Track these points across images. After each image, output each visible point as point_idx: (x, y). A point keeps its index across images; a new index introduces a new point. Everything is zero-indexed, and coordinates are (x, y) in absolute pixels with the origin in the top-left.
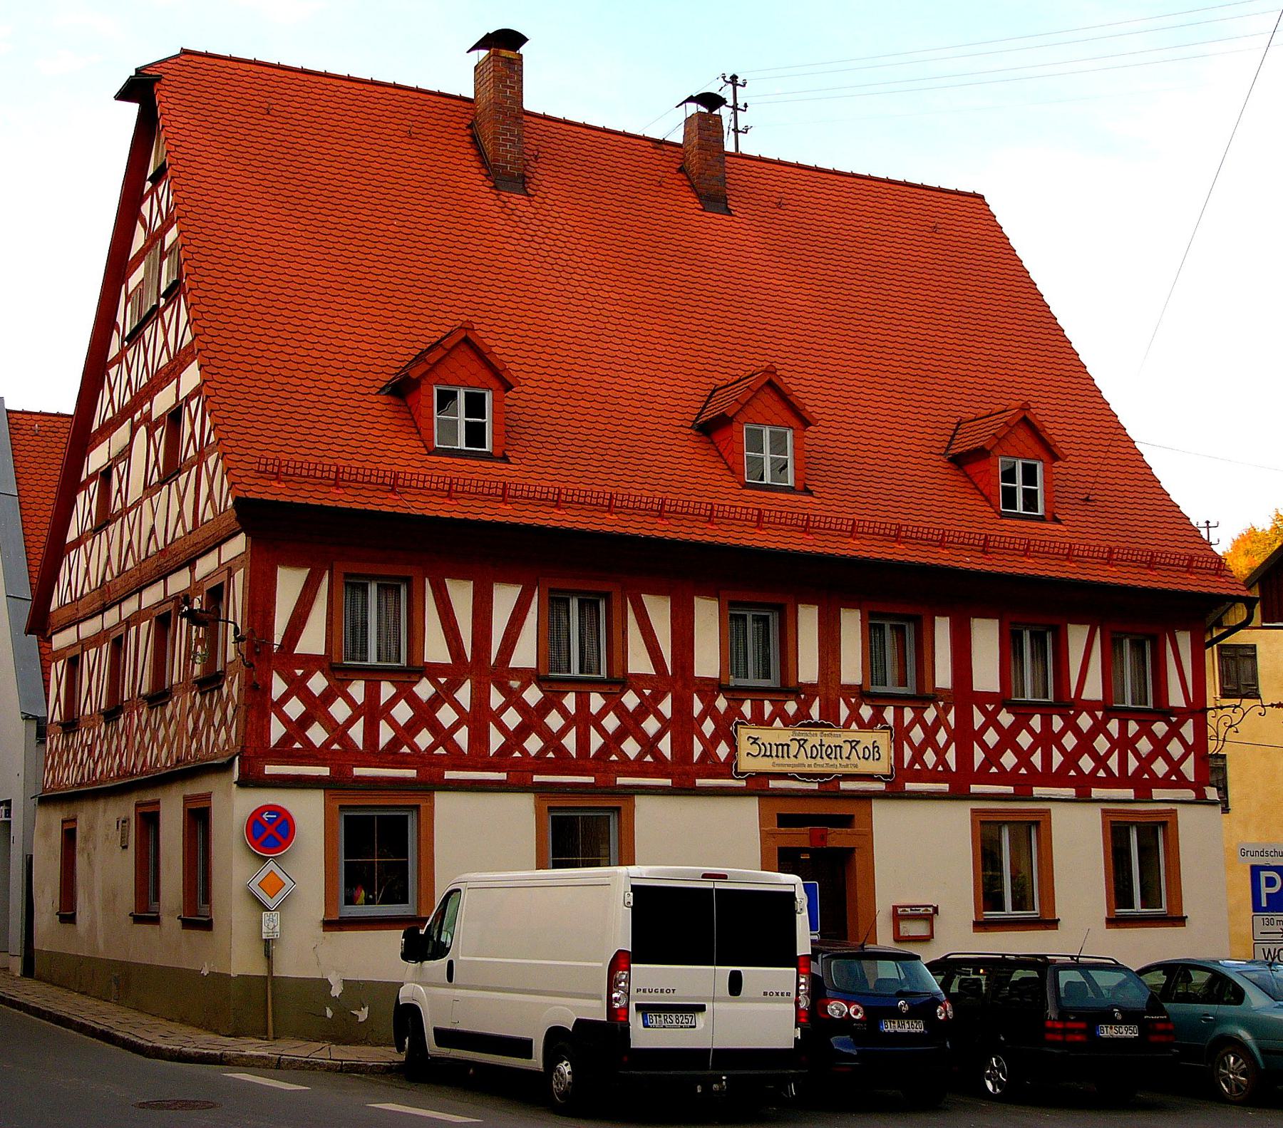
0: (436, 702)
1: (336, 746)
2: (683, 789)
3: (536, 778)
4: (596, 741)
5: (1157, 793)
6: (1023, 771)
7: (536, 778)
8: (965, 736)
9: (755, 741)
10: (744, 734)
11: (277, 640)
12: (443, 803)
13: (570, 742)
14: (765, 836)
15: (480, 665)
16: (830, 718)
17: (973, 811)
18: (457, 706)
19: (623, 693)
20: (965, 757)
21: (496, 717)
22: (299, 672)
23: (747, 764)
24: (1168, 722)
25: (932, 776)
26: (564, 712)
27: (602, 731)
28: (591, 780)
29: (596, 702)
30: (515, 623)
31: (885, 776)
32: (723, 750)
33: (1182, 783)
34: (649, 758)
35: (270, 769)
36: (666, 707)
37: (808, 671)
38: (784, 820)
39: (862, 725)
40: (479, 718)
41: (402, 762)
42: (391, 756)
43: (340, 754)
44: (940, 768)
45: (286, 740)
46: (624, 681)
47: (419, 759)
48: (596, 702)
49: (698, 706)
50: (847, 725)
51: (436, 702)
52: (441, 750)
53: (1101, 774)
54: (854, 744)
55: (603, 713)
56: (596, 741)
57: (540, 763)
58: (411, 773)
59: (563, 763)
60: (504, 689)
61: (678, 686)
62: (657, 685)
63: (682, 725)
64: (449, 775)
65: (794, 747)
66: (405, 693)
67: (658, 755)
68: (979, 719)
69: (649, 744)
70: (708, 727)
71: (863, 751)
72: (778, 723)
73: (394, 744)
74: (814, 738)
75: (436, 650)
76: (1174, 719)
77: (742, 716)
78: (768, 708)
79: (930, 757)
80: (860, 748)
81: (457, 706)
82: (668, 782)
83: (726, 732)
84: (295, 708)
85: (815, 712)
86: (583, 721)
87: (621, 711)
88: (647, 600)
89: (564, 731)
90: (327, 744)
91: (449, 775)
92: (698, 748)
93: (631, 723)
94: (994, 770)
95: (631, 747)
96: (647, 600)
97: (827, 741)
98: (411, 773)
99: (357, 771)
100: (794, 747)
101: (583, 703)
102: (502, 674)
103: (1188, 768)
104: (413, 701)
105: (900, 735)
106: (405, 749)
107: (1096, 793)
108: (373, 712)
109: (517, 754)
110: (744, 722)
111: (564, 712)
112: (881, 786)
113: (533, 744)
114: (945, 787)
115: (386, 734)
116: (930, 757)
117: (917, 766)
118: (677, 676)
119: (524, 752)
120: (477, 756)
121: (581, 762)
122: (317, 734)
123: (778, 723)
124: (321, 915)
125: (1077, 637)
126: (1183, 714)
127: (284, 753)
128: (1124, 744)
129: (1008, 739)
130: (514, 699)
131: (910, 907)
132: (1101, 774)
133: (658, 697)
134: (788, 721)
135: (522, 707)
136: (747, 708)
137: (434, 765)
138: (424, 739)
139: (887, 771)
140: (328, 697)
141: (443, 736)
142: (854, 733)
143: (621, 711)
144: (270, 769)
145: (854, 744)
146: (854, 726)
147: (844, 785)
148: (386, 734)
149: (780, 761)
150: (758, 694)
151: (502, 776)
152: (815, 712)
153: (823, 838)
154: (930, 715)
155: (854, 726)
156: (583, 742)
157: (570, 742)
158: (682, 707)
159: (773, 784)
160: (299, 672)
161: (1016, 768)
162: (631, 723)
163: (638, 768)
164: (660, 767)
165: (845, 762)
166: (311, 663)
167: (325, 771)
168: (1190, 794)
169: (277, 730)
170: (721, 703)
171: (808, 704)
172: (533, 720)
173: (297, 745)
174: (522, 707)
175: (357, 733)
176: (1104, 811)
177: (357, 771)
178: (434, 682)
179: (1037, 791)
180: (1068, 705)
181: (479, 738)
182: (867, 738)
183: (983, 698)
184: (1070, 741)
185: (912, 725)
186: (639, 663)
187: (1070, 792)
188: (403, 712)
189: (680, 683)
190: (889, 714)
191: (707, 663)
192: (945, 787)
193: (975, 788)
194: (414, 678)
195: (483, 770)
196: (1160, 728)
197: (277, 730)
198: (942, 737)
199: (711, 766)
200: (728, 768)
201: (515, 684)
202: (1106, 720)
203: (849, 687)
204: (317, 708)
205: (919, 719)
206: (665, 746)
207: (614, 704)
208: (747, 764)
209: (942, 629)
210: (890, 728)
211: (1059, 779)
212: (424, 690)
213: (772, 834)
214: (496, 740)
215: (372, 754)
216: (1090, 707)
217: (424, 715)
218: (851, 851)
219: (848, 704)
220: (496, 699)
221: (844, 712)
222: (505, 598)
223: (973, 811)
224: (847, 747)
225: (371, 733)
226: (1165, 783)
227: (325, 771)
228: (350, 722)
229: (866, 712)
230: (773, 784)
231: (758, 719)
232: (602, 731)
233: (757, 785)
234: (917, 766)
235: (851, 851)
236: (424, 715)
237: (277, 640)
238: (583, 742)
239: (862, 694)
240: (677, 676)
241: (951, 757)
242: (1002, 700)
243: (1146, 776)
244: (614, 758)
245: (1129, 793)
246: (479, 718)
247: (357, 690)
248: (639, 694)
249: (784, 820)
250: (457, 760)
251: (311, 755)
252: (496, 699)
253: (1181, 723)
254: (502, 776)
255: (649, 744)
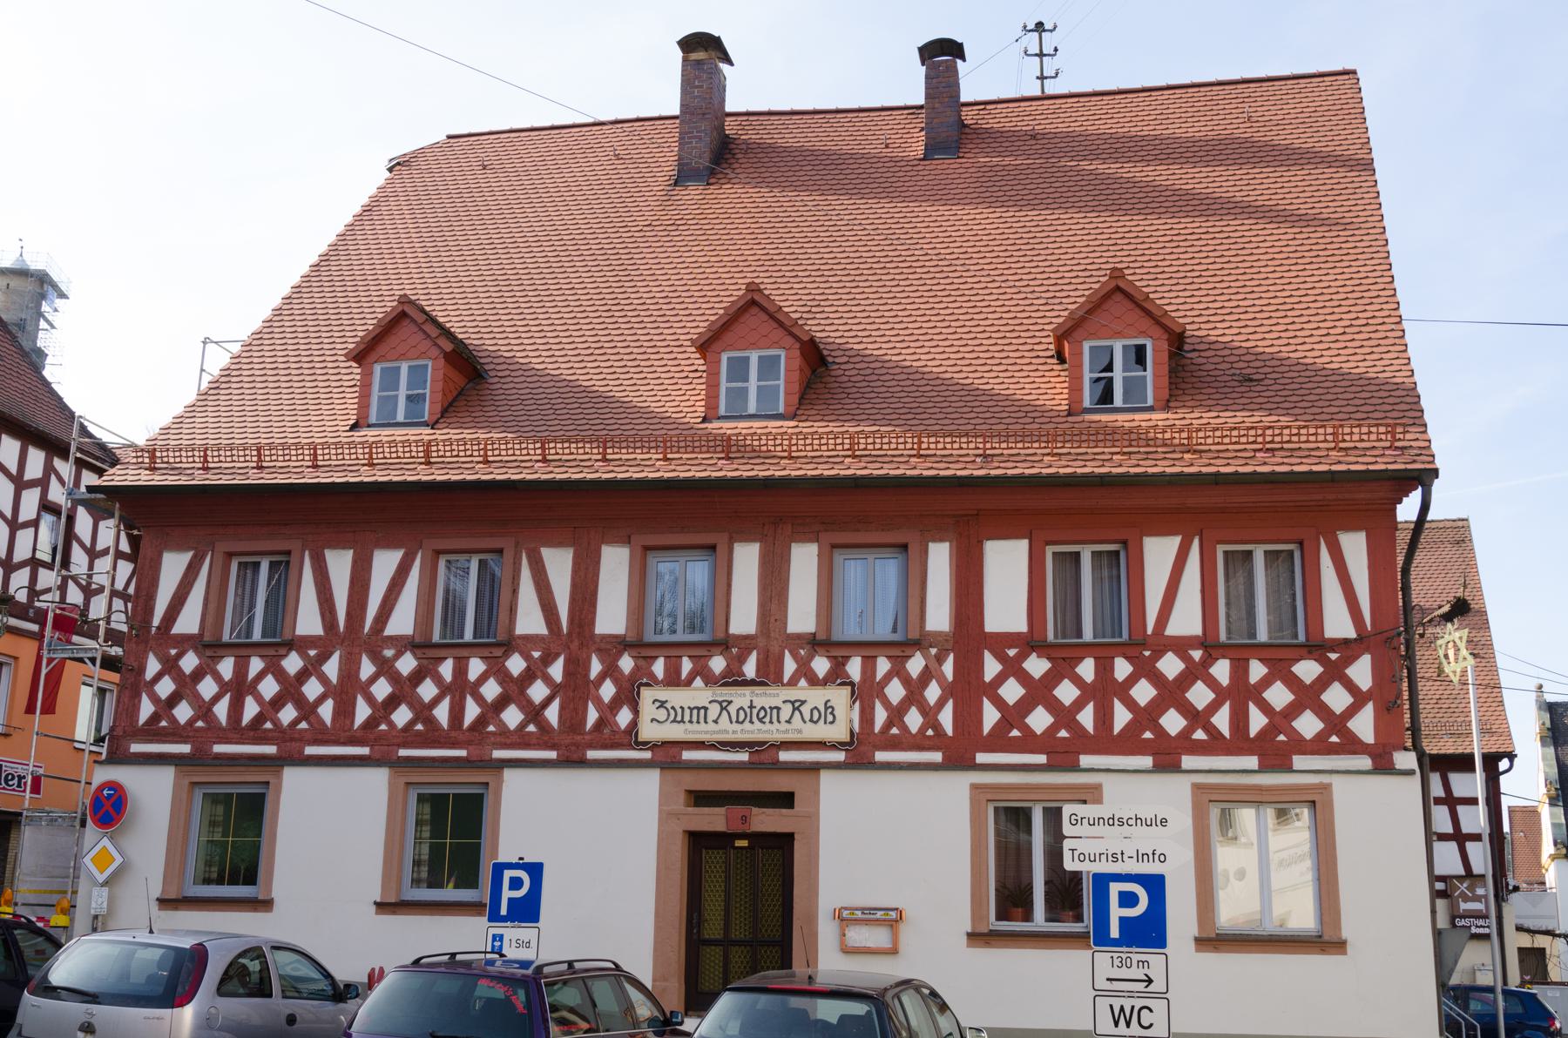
0: (303, 676)
1: (200, 724)
2: (572, 759)
3: (403, 752)
4: (472, 711)
5: (1299, 762)
6: (1063, 734)
7: (403, 752)
8: (968, 691)
9: (662, 704)
10: (647, 695)
11: (156, 622)
12: (294, 781)
13: (442, 713)
14: (665, 817)
15: (354, 635)
16: (769, 675)
17: (975, 787)
18: (324, 680)
19: (507, 655)
20: (968, 717)
21: (365, 689)
22: (173, 652)
23: (648, 732)
24: (1323, 661)
25: (918, 743)
26: (438, 680)
27: (479, 699)
28: (462, 753)
29: (476, 667)
30: (396, 587)
31: (842, 744)
32: (624, 717)
33: (1352, 745)
34: (531, 728)
35: (136, 748)
36: (557, 671)
37: (744, 618)
38: (701, 798)
39: (814, 681)
40: (346, 691)
41: (263, 739)
42: (255, 732)
43: (204, 731)
44: (930, 732)
45: (155, 718)
46: (510, 644)
47: (283, 736)
48: (476, 667)
49: (596, 667)
50: (793, 682)
51: (303, 676)
52: (303, 725)
53: (1200, 735)
54: (724, 706)
55: (483, 679)
56: (472, 711)
57: (408, 736)
58: (270, 749)
59: (433, 736)
60: (376, 657)
61: (575, 645)
62: (549, 647)
63: (575, 690)
64: (310, 750)
65: (714, 710)
66: (273, 668)
67: (544, 726)
68: (992, 667)
69: (535, 713)
70: (608, 691)
71: (815, 712)
72: (698, 682)
73: (259, 719)
74: (741, 698)
75: (309, 622)
76: (1333, 656)
77: (652, 676)
78: (687, 666)
79: (914, 720)
80: (806, 709)
81: (324, 680)
82: (552, 755)
83: (629, 695)
84: (165, 688)
85: (750, 669)
86: (460, 688)
87: (503, 676)
88: (546, 553)
89: (436, 701)
90: (191, 722)
91: (310, 750)
92: (592, 715)
93: (514, 691)
94: (1015, 733)
95: (512, 717)
96: (546, 553)
97: (758, 703)
98: (270, 749)
99: (219, 749)
100: (714, 710)
101: (461, 670)
102: (375, 645)
103: (1364, 725)
104: (280, 675)
105: (867, 693)
106: (268, 725)
107: (1188, 761)
108: (240, 688)
109: (383, 727)
110: (653, 682)
111: (438, 680)
112: (840, 756)
113: (402, 716)
114: (937, 757)
115: (251, 709)
116: (914, 720)
117: (895, 731)
118: (575, 636)
119: (391, 724)
120: (342, 732)
121: (453, 734)
122: (183, 712)
123: (698, 682)
124: (157, 892)
125: (1159, 552)
126: (1350, 650)
127: (151, 731)
128: (1241, 694)
129: (1039, 692)
130: (385, 668)
131: (863, 910)
132: (1200, 735)
133: (548, 660)
134: (710, 680)
135: (394, 677)
136: (659, 668)
137: (292, 740)
138: (288, 714)
139: (845, 737)
140: (198, 675)
141: (307, 710)
142: (802, 691)
143: (503, 676)
144: (136, 748)
145: (797, 705)
146: (803, 683)
147: (785, 756)
148: (251, 709)
149: (695, 727)
150: (673, 649)
151: (365, 751)
152: (750, 669)
153: (745, 819)
154: (915, 665)
155: (803, 683)
156: (457, 713)
157: (442, 713)
158: (576, 669)
159: (687, 755)
160: (173, 652)
161: (1052, 729)
162: (514, 691)
163: (519, 739)
164: (546, 737)
165: (784, 726)
166: (186, 642)
167: (185, 749)
168: (1365, 762)
169: (146, 709)
170: (626, 664)
171: (742, 660)
172: (404, 691)
173: (164, 723)
174: (394, 677)
175: (221, 710)
176: (1197, 788)
177: (219, 749)
178: (303, 655)
179: (1086, 760)
180: (1144, 648)
181: (345, 710)
182: (815, 697)
183: (998, 643)
184: (1144, 692)
185: (888, 678)
186: (530, 621)
187: (1147, 761)
188: (269, 687)
189: (576, 643)
190: (854, 668)
191: (611, 618)
192: (937, 757)
193: (981, 758)
194: (282, 651)
195: (344, 744)
196: (1308, 670)
197: (146, 709)
198: (933, 693)
199: (607, 735)
200: (630, 737)
201: (389, 653)
202: (1209, 660)
203: (799, 636)
204: (186, 686)
205: (898, 671)
206: (552, 714)
207: (496, 669)
208: (648, 732)
209: (940, 556)
210: (852, 684)
211: (1128, 743)
212: (293, 663)
213: (677, 815)
214: (362, 712)
215: (236, 731)
216: (1180, 646)
217: (291, 690)
218: (790, 837)
219: (795, 656)
220: (367, 669)
221: (790, 666)
222: (385, 562)
223: (975, 787)
224: (787, 710)
225: (236, 709)
226: (1319, 746)
227: (185, 749)
228: (216, 699)
229: (821, 665)
230: (687, 755)
231: (673, 679)
232: (479, 699)
233: (666, 756)
234: (895, 731)
235: (790, 837)
236: (291, 690)
237: (156, 622)
238: (457, 713)
239: (816, 643)
240: (575, 636)
241: (946, 718)
242: (1031, 642)
243: (1282, 738)
244: (491, 728)
245: (1252, 762)
246: (346, 691)
247: (226, 668)
248: (527, 657)
249: (701, 798)
250: (321, 735)
251: (177, 733)
252: (367, 669)
253: (1349, 660)
254: (364, 751)
255: (535, 713)
